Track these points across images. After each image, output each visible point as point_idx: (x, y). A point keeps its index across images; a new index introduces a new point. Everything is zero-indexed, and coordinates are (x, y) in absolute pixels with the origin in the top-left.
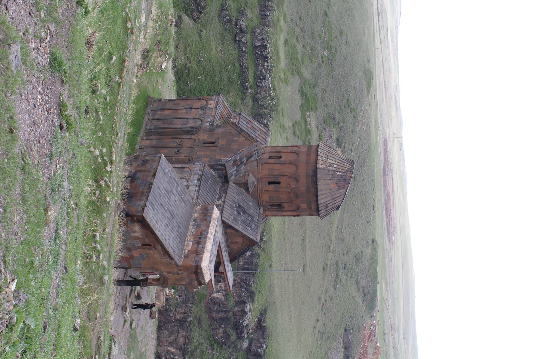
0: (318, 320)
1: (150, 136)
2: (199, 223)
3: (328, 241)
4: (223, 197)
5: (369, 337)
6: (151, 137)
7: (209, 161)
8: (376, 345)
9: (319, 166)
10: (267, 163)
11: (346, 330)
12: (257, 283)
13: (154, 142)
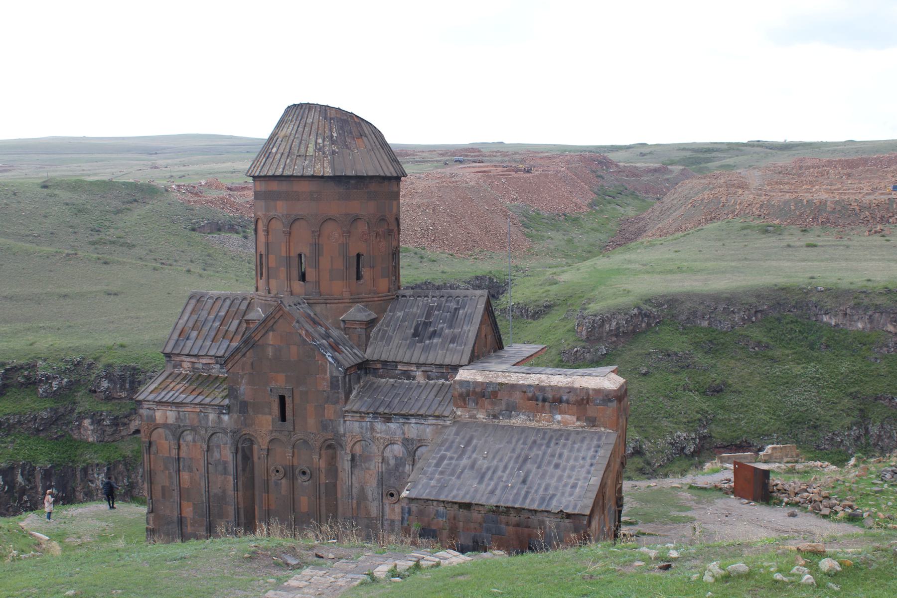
0: (189, 271)
2: (504, 407)
4: (406, 368)
5: (196, 194)
8: (204, 186)
9: (328, 172)
10: (318, 283)
11: (194, 230)
12: (156, 366)
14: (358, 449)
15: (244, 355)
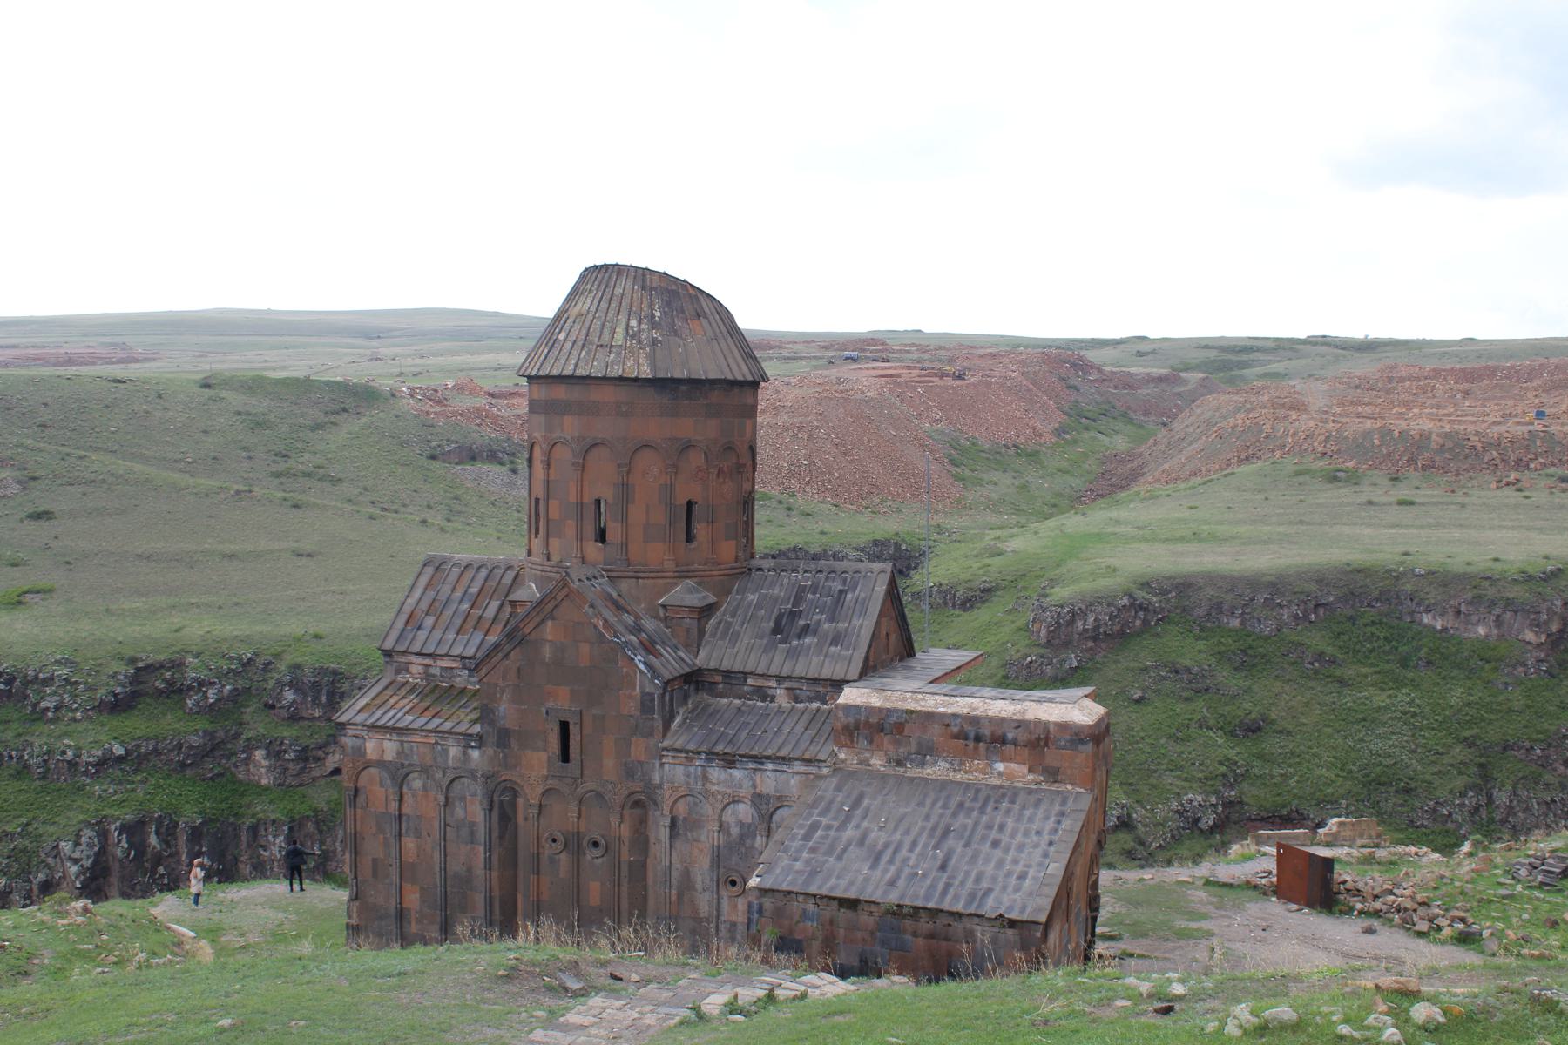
0: (424, 522)
2: (913, 748)
5: (439, 402)
9: (646, 372)
10: (625, 545)
11: (433, 457)
12: (369, 669)
14: (681, 809)
15: (506, 656)
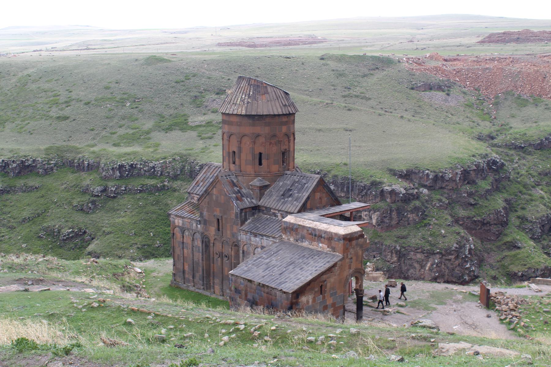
0: (402, 117)
1: (210, 286)
2: (300, 236)
3: (321, 105)
5: (420, 64)
6: (212, 284)
7: (237, 225)
8: (428, 58)
9: (244, 113)
10: (240, 166)
11: (412, 89)
12: (363, 179)
13: (217, 281)
